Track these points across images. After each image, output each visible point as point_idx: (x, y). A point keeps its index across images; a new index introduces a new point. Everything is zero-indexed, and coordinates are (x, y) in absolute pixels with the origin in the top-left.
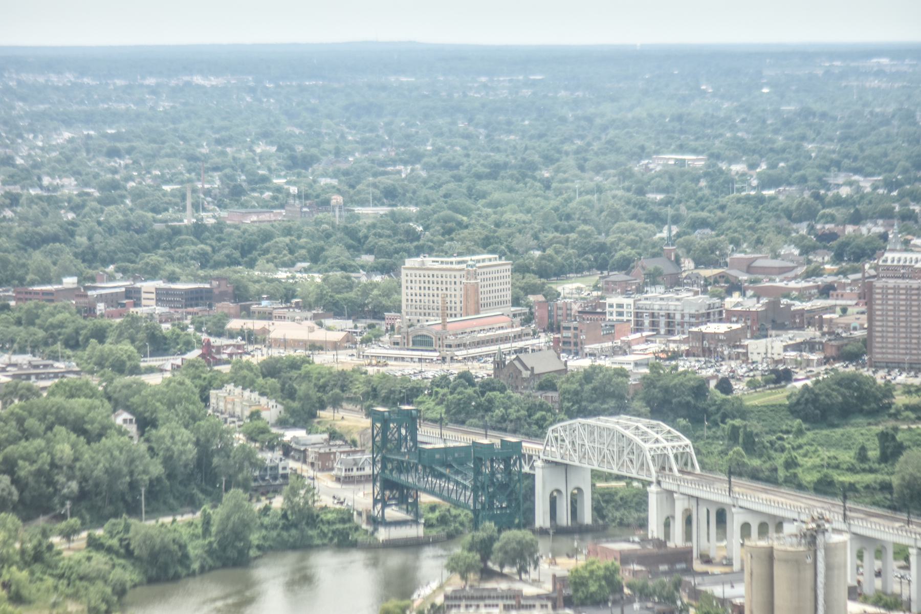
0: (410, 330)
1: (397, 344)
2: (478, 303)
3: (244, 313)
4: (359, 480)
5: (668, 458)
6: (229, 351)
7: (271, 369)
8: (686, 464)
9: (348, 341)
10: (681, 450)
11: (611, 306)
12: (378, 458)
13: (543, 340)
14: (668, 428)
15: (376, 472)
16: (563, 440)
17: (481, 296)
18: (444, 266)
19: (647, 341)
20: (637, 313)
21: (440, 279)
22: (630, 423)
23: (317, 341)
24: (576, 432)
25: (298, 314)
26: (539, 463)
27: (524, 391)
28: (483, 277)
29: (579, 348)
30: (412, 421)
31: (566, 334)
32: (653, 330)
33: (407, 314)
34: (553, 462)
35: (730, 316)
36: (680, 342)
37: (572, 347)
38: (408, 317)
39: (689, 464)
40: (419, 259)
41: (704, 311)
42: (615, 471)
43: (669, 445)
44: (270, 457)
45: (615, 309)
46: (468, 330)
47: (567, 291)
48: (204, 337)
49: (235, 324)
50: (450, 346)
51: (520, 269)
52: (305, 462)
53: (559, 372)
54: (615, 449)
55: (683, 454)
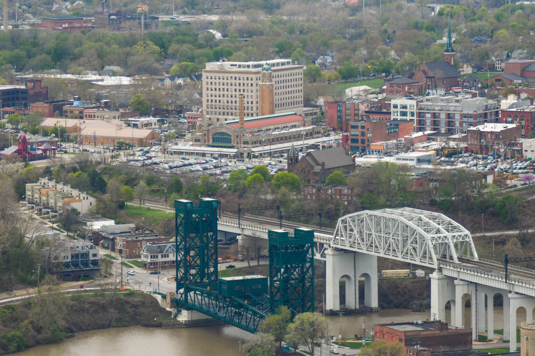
0: (210, 127)
3: (57, 112)
8: (465, 253)
9: (153, 138)
10: (461, 240)
11: (395, 107)
12: (181, 246)
13: (334, 138)
14: (449, 219)
15: (179, 259)
16: (352, 230)
18: (242, 69)
19: (429, 139)
20: (420, 113)
21: (238, 82)
22: (413, 215)
25: (107, 113)
26: (329, 252)
28: (277, 79)
29: (365, 145)
31: (353, 132)
32: (434, 129)
33: (208, 113)
34: (342, 250)
35: (507, 116)
36: (459, 140)
37: (359, 144)
38: (208, 116)
39: (468, 253)
40: (218, 63)
41: (482, 112)
42: (400, 259)
43: (449, 235)
45: (399, 109)
46: (264, 129)
47: (355, 92)
49: (49, 122)
52: (113, 250)
54: (400, 238)
55: (462, 243)
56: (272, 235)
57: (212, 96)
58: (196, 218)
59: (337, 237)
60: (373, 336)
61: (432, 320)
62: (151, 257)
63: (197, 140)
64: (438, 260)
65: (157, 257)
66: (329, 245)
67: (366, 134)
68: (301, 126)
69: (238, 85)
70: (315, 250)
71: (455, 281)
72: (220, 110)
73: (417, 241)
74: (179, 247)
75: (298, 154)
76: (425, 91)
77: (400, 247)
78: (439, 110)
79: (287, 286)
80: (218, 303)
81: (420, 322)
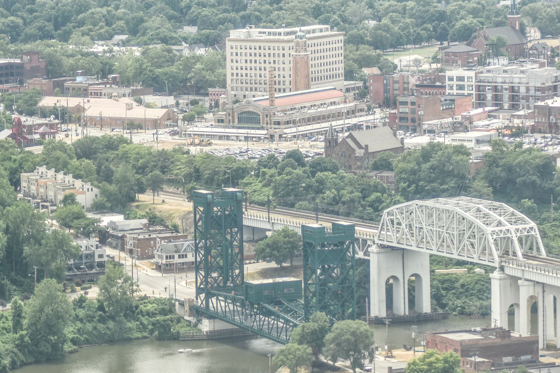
0: (235, 106)
1: (222, 121)
2: (308, 76)
3: (57, 89)
4: (182, 268)
5: (512, 242)
6: (41, 130)
7: (86, 150)
8: (531, 249)
9: (168, 119)
10: (526, 233)
11: (451, 79)
14: (512, 209)
15: (199, 259)
17: (311, 70)
18: (272, 37)
19: (489, 116)
20: (479, 86)
21: (267, 52)
22: (471, 205)
23: (136, 119)
24: (414, 215)
25: (116, 90)
26: (373, 249)
27: (357, 171)
28: (313, 48)
29: (416, 124)
30: (237, 204)
32: (496, 105)
33: (232, 90)
34: (388, 247)
36: (525, 117)
37: (409, 123)
38: (233, 93)
41: (551, 84)
42: (455, 256)
43: (512, 228)
44: (85, 244)
45: (455, 83)
46: (298, 106)
47: (404, 63)
48: (15, 116)
49: (48, 102)
50: (279, 123)
51: (354, 41)
52: (123, 249)
53: (395, 150)
54: (455, 233)
56: (306, 231)
57: (237, 69)
58: (218, 212)
59: (382, 232)
60: (424, 346)
61: (493, 326)
62: (167, 258)
63: (221, 121)
64: (499, 257)
65: (173, 257)
66: (374, 242)
67: (417, 112)
68: (342, 103)
69: (267, 55)
70: (357, 247)
71: (519, 281)
72: (246, 85)
73: (475, 236)
74: (199, 246)
75: (337, 136)
76: (485, 59)
77: (455, 242)
78: (502, 83)
79: (325, 289)
80: (244, 310)
81: (478, 329)
